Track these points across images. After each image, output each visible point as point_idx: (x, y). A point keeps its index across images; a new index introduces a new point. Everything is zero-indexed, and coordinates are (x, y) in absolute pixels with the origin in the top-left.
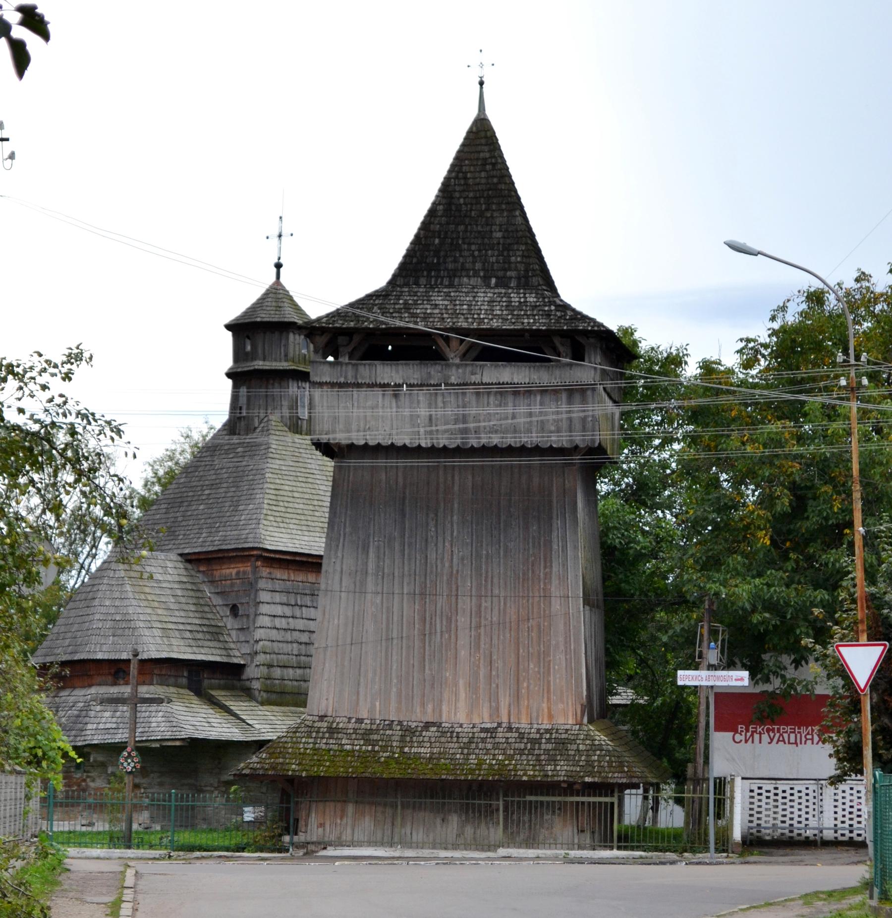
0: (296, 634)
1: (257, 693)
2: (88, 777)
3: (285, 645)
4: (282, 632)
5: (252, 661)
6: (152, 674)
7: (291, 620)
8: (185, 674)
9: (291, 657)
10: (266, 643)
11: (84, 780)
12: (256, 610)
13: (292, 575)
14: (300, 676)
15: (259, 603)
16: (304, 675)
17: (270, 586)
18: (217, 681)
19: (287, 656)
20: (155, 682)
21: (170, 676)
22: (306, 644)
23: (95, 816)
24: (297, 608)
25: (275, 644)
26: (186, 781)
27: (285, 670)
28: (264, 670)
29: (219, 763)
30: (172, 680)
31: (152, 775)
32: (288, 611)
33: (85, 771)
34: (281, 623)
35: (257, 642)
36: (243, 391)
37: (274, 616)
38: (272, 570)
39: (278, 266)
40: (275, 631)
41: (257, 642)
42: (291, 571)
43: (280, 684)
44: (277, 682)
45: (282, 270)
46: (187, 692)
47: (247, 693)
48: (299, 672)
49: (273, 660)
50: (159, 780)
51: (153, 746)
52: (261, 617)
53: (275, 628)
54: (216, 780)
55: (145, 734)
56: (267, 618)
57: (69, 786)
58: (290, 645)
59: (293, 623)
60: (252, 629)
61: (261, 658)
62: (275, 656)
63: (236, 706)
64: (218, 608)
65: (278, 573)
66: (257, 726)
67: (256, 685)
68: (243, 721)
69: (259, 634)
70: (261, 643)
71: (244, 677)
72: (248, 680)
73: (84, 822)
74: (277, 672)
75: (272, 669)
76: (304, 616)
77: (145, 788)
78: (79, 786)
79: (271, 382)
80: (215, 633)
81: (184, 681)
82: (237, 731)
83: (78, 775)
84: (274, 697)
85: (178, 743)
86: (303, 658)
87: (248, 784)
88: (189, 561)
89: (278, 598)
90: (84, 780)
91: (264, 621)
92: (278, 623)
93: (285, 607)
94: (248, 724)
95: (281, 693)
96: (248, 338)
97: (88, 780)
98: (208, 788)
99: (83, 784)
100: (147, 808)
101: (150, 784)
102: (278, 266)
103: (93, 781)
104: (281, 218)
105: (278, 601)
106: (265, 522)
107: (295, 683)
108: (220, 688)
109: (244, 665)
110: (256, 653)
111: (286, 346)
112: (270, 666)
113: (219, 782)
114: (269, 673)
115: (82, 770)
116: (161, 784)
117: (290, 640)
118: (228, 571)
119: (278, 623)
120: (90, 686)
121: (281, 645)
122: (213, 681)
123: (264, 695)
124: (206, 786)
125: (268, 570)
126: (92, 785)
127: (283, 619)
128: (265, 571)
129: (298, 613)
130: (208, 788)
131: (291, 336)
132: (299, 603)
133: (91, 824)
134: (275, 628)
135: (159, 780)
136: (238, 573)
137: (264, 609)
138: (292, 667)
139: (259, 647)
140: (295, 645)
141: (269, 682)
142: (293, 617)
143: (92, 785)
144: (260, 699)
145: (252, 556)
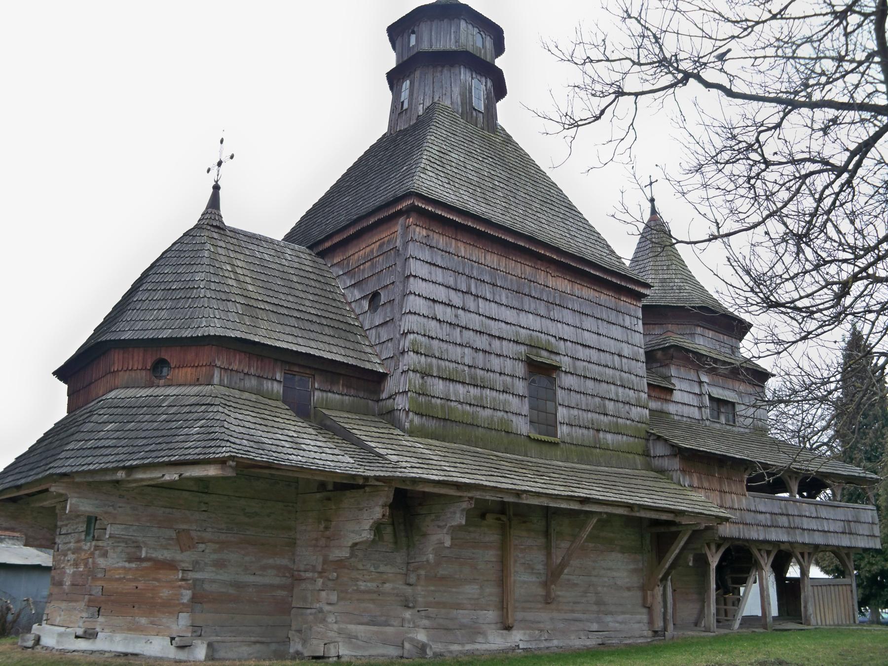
0: (468, 335)
1: (403, 415)
2: (97, 548)
3: (451, 347)
4: (446, 328)
5: (397, 367)
6: (212, 366)
7: (460, 312)
8: (278, 376)
9: (461, 367)
10: (419, 338)
11: (92, 554)
12: (405, 287)
13: (463, 249)
14: (475, 397)
15: (408, 277)
16: (481, 398)
17: (426, 255)
18: (337, 396)
19: (454, 365)
20: (216, 380)
21: (247, 374)
22: (485, 352)
23: (101, 619)
24: (472, 298)
25: (435, 343)
26: (271, 561)
27: (451, 385)
28: (416, 379)
29: (327, 528)
30: (253, 382)
31: (202, 547)
32: (456, 299)
34: (445, 313)
35: (405, 334)
36: (407, 84)
37: (434, 301)
38: (431, 233)
40: (434, 323)
41: (405, 334)
42: (459, 244)
43: (442, 406)
44: (439, 401)
46: (280, 404)
47: (389, 417)
48: (474, 391)
49: (430, 366)
50: (215, 556)
51: (167, 478)
52: (412, 297)
53: (434, 318)
54: (321, 559)
55: (154, 454)
56: (420, 302)
58: (459, 349)
59: (464, 318)
60: (397, 316)
61: (411, 359)
62: (434, 361)
63: (362, 431)
64: (353, 305)
65: (440, 241)
66: (389, 457)
67: (401, 403)
68: (371, 450)
69: (409, 323)
70: (411, 337)
71: (384, 396)
72: (390, 398)
74: (438, 387)
75: (429, 380)
76: (481, 311)
77: (184, 570)
79: (440, 69)
80: (345, 330)
81: (278, 388)
82: (347, 459)
84: (431, 424)
85: (212, 471)
86: (480, 373)
87: (382, 568)
88: (322, 254)
89: (439, 275)
91: (414, 303)
92: (440, 311)
93: (452, 293)
94: (380, 455)
95: (445, 419)
96: (413, 32)
97: (97, 552)
98: (309, 575)
100: (184, 608)
101: (196, 563)
103: (105, 555)
105: (440, 280)
106: (422, 175)
107: (468, 407)
108: (342, 408)
109: (386, 374)
110: (403, 353)
111: (458, 31)
112: (425, 374)
113: (325, 562)
114: (423, 385)
116: (220, 565)
117: (459, 341)
118: (368, 249)
119: (440, 311)
121: (444, 346)
122: (330, 395)
123: (417, 420)
125: (424, 232)
127: (449, 309)
128: (420, 232)
129: (471, 303)
130: (309, 575)
131: (463, 24)
132: (474, 291)
133: (90, 635)
134: (434, 318)
135: (215, 556)
136: (381, 246)
137: (415, 285)
138: (463, 383)
139: (406, 343)
140: (466, 350)
141: (422, 399)
142: (463, 309)
143: (102, 562)
144: (407, 425)
145: (400, 213)
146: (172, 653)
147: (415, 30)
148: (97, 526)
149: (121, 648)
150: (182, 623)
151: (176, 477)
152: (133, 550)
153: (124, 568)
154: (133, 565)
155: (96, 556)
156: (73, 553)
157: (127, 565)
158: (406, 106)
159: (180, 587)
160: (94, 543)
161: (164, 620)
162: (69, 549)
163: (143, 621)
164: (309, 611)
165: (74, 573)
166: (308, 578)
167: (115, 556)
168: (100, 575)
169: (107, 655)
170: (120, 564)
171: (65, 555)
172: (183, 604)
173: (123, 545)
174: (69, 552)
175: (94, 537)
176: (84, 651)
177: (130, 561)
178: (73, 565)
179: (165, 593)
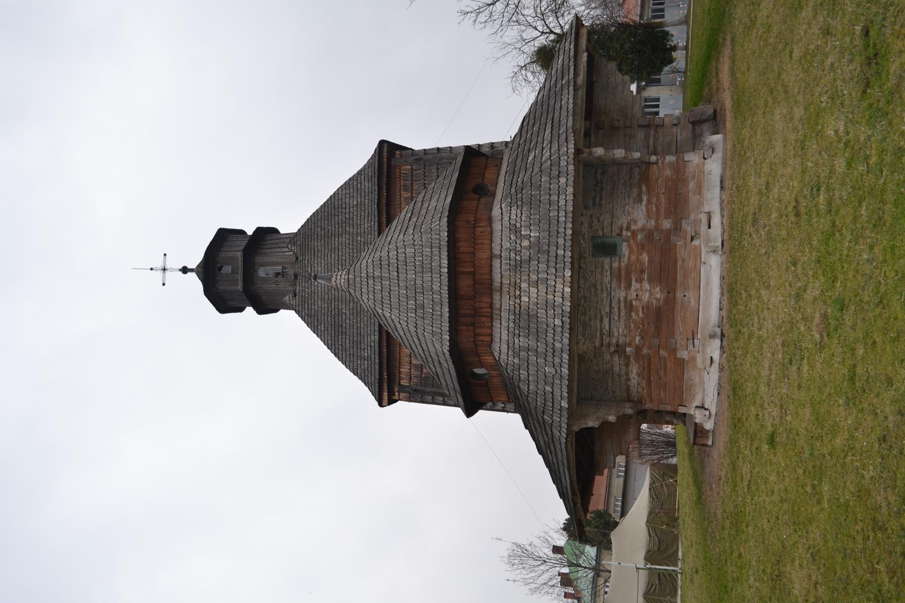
11: (634, 234)
33: (619, 235)
36: (261, 272)
39: (185, 270)
45: (189, 267)
57: (642, 271)
73: (704, 226)
78: (641, 247)
83: (625, 249)
90: (634, 234)
96: (220, 269)
97: (633, 227)
99: (639, 237)
102: (185, 270)
103: (635, 222)
104: (152, 269)
115: (617, 240)
120: (490, 220)
124: (648, 147)
126: (640, 224)
146: (718, 155)
147: (219, 265)
148: (609, 234)
149: (718, 189)
150: (693, 158)
151: (585, 54)
152: (631, 199)
153: (647, 205)
154: (645, 198)
155: (636, 228)
156: (629, 286)
157: (644, 203)
158: (279, 268)
159: (663, 163)
160: (624, 233)
161: (691, 170)
162: (626, 298)
163: (692, 185)
164: (679, 138)
165: (650, 281)
166: (654, 142)
167: (636, 213)
168: (653, 223)
169: (723, 198)
170: (644, 208)
171: (630, 307)
172: (677, 160)
173: (627, 207)
174: (629, 298)
175: (618, 235)
176: (722, 216)
177: (641, 201)
178: (641, 282)
179: (668, 172)
